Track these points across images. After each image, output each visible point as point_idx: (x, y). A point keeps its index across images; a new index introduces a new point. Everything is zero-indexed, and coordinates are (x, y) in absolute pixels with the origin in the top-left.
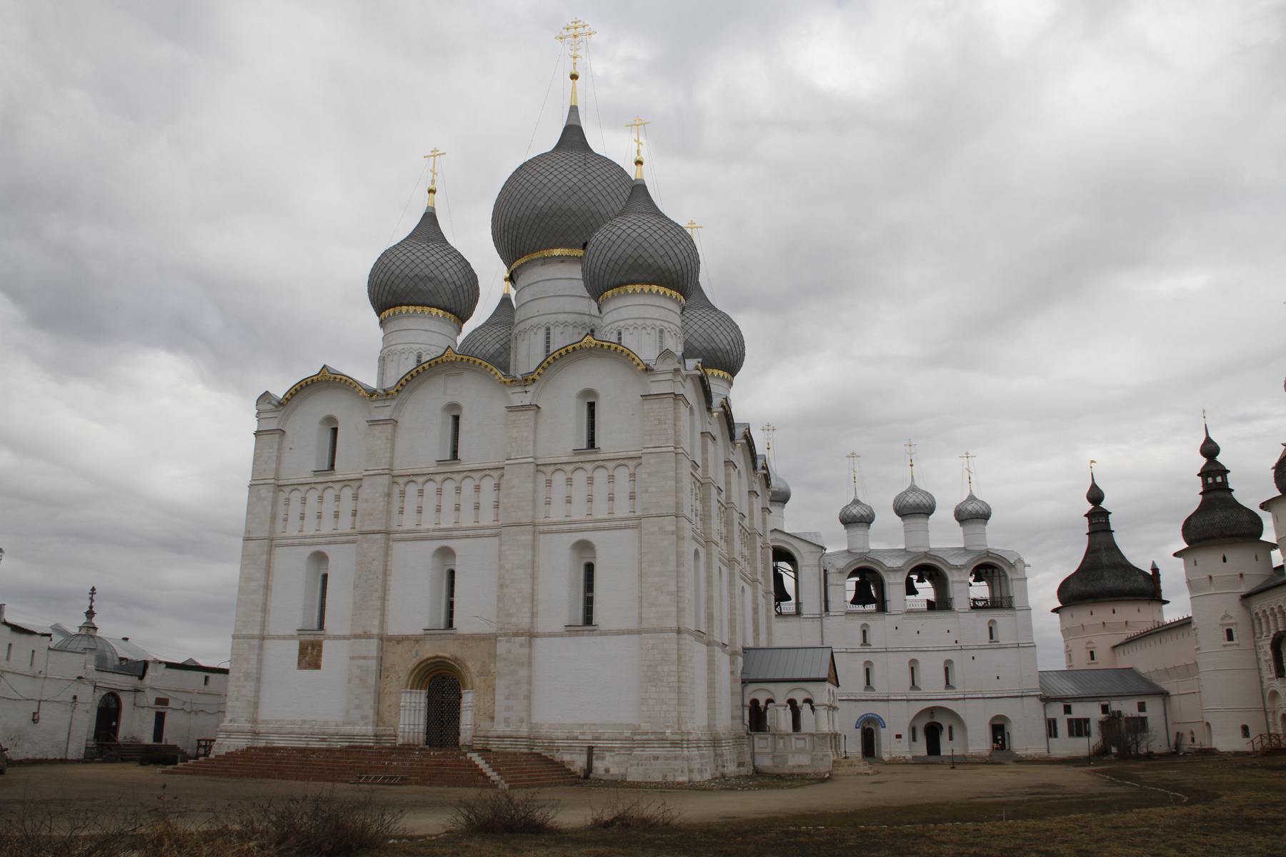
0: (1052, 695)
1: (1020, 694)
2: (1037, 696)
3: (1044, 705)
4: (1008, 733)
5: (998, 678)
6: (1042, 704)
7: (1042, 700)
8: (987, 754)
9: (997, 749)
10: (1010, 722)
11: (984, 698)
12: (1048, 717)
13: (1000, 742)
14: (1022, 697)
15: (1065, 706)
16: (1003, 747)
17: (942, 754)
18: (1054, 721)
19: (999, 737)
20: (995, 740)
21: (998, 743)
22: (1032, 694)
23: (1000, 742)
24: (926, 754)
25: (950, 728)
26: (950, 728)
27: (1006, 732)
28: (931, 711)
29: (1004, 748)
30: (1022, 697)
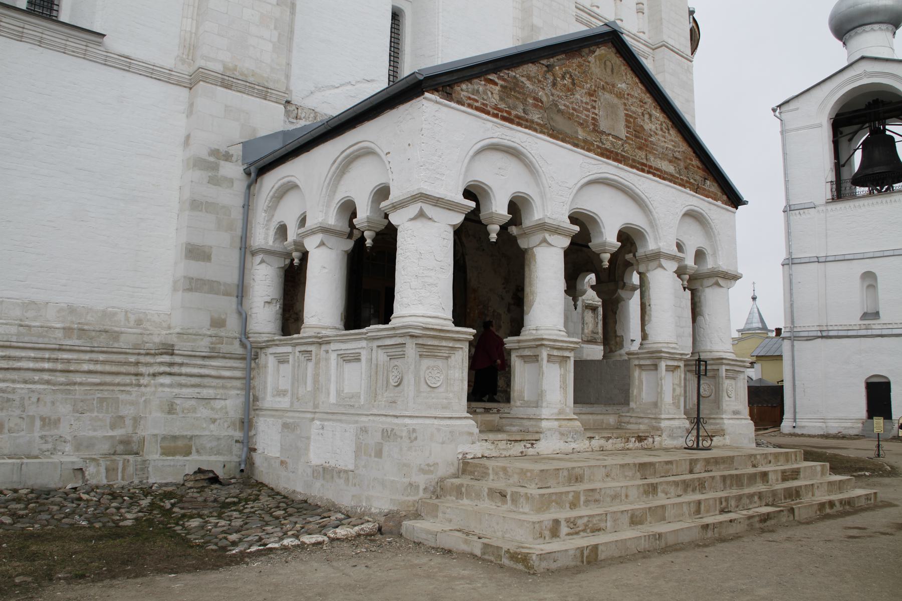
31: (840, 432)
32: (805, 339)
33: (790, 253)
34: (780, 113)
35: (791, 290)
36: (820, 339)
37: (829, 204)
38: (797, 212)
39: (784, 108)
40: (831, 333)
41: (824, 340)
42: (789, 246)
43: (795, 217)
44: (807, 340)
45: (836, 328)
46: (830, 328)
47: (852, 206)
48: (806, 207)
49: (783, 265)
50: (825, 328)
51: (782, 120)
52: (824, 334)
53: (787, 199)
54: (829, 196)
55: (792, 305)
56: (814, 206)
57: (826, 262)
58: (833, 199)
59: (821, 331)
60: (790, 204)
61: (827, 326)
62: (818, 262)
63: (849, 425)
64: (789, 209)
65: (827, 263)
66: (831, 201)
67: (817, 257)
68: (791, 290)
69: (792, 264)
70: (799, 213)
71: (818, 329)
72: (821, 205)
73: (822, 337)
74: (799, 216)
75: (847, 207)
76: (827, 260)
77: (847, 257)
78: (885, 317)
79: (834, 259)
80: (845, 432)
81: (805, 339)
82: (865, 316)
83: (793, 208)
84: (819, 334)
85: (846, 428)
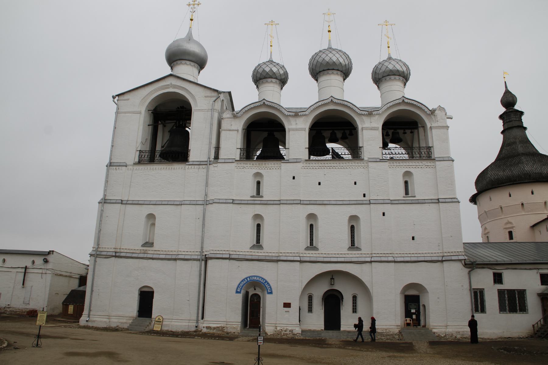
0: (479, 261)
1: (440, 259)
2: (460, 260)
3: (469, 273)
4: (424, 306)
5: (413, 238)
6: (467, 270)
7: (466, 265)
8: (397, 331)
9: (408, 324)
10: (427, 292)
11: (395, 262)
12: (474, 286)
13: (414, 317)
14: (442, 261)
15: (495, 274)
16: (417, 322)
17: (342, 329)
18: (482, 291)
19: (413, 311)
20: (408, 314)
21: (411, 317)
22: (453, 258)
23: (414, 317)
24: (323, 328)
25: (355, 298)
26: (355, 298)
27: (421, 305)
28: (332, 275)
29: (419, 324)
30: (442, 261)
31: (118, 326)
32: (105, 257)
33: (105, 195)
34: (118, 100)
35: (101, 221)
36: (114, 258)
37: (135, 165)
38: (115, 167)
39: (121, 98)
40: (122, 254)
41: (117, 259)
42: (105, 190)
43: (113, 170)
44: (105, 258)
45: (125, 251)
46: (122, 251)
47: (149, 168)
48: (121, 165)
49: (99, 203)
50: (118, 251)
51: (117, 105)
52: (117, 254)
53: (111, 159)
54: (137, 160)
55: (100, 230)
56: (125, 165)
57: (126, 204)
58: (139, 162)
59: (115, 252)
60: (111, 162)
61: (120, 249)
62: (122, 203)
63: (124, 321)
64: (110, 165)
65: (128, 206)
66: (137, 163)
67: (122, 200)
68: (101, 221)
69: (104, 203)
70: (116, 169)
71: (114, 250)
72: (131, 165)
73: (116, 256)
74: (115, 171)
75: (146, 168)
76: (127, 203)
77: (140, 202)
78: (156, 247)
79: (131, 203)
80: (121, 326)
81: (105, 257)
82: (144, 245)
83: (112, 165)
84: (114, 254)
85: (122, 323)
